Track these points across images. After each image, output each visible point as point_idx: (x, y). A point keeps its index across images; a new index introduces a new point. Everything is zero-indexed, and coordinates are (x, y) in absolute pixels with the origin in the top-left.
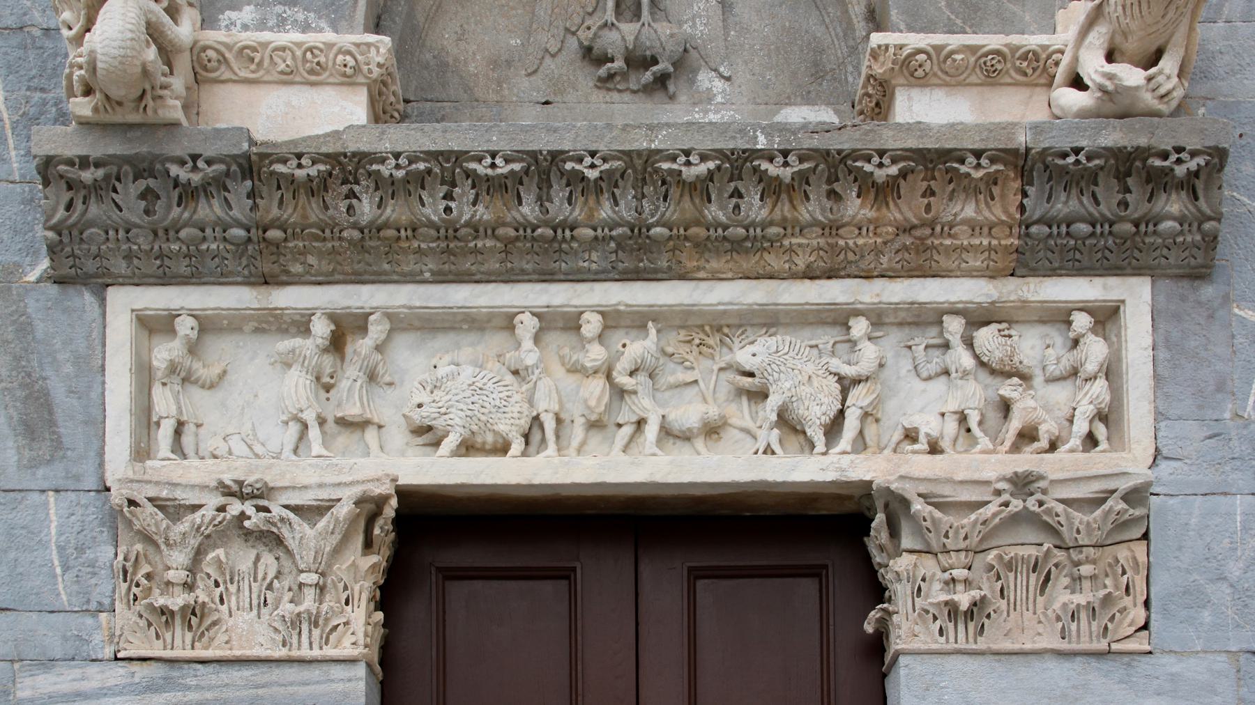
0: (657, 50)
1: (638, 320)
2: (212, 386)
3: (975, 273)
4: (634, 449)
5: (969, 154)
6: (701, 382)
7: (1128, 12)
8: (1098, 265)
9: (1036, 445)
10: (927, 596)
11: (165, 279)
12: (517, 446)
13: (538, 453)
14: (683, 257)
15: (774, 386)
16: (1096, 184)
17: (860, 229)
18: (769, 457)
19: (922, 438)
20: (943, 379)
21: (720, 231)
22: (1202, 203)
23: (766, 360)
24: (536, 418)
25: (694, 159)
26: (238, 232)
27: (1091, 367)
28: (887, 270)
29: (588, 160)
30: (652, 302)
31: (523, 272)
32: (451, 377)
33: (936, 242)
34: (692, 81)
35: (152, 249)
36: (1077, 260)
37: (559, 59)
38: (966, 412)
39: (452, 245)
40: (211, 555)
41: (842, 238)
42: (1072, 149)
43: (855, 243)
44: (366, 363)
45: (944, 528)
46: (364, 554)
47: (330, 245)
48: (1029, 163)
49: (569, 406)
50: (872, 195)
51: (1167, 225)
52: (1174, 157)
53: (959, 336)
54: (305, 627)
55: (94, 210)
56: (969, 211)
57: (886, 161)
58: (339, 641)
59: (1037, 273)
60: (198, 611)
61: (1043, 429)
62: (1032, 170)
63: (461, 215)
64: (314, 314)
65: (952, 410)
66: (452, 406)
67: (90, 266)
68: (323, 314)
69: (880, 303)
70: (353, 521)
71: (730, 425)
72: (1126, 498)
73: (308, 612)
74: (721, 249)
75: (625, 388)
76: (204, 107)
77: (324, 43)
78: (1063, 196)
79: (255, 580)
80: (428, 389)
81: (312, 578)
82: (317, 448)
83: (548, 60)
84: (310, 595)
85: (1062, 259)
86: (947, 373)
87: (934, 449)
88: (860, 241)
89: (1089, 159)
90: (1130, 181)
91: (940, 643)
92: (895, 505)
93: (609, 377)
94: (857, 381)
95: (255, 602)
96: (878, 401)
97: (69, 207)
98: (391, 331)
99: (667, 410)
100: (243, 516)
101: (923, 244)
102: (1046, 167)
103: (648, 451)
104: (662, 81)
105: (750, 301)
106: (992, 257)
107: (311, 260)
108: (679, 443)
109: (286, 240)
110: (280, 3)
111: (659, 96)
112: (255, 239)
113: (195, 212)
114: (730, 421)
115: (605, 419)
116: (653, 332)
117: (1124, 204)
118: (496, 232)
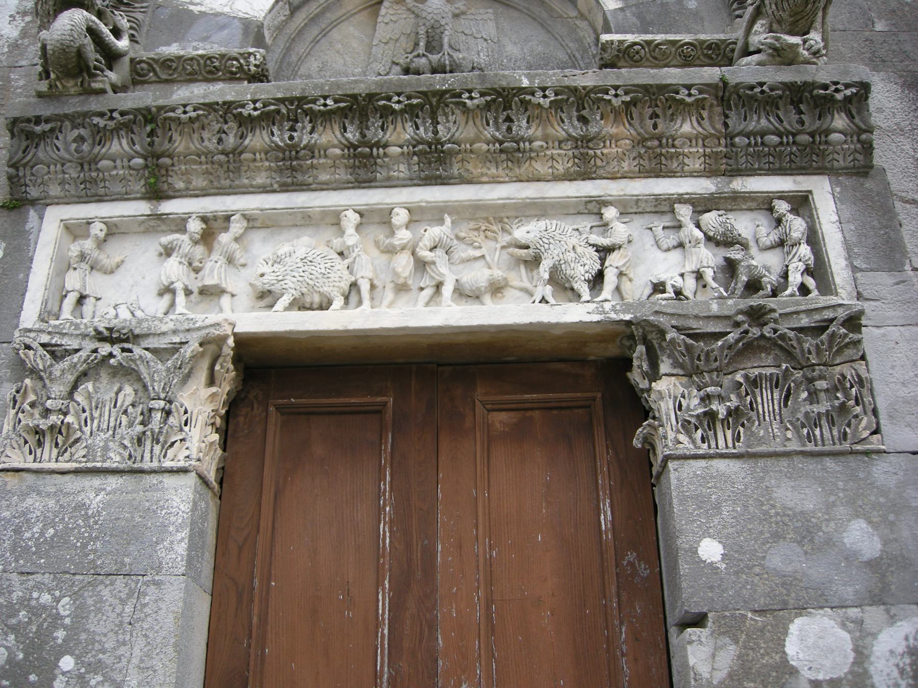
1: (436, 213)
2: (112, 272)
3: (696, 174)
5: (681, 88)
6: (488, 258)
7: (780, 7)
9: (761, 293)
12: (338, 302)
13: (357, 307)
14: (470, 167)
15: (546, 254)
16: (778, 109)
17: (604, 142)
18: (543, 305)
19: (669, 288)
20: (679, 251)
21: (497, 145)
23: (538, 235)
28: (626, 172)
29: (396, 98)
30: (446, 199)
32: (288, 255)
33: (664, 151)
35: (79, 176)
36: (771, 163)
38: (701, 270)
39: (294, 163)
41: (592, 149)
42: (757, 83)
43: (602, 153)
44: (225, 249)
47: (204, 167)
48: (727, 94)
50: (612, 116)
52: (833, 88)
53: (689, 218)
54: (148, 444)
56: (687, 128)
59: (742, 173)
60: (64, 431)
62: (729, 100)
63: (301, 140)
64: (190, 217)
65: (690, 270)
66: (287, 275)
68: (197, 217)
69: (625, 195)
71: (512, 287)
74: (498, 159)
75: (426, 260)
77: (219, 55)
79: (115, 406)
80: (270, 264)
85: (759, 163)
86: (681, 245)
89: (772, 90)
90: (802, 107)
92: (653, 337)
95: (112, 424)
98: (247, 229)
99: (460, 276)
100: (111, 355)
101: (653, 152)
102: (740, 97)
103: (443, 304)
105: (524, 196)
106: (707, 161)
109: (173, 165)
110: (196, 41)
112: (150, 164)
113: (109, 148)
114: (510, 283)
115: (410, 282)
116: (448, 220)
117: (802, 123)
118: (327, 152)
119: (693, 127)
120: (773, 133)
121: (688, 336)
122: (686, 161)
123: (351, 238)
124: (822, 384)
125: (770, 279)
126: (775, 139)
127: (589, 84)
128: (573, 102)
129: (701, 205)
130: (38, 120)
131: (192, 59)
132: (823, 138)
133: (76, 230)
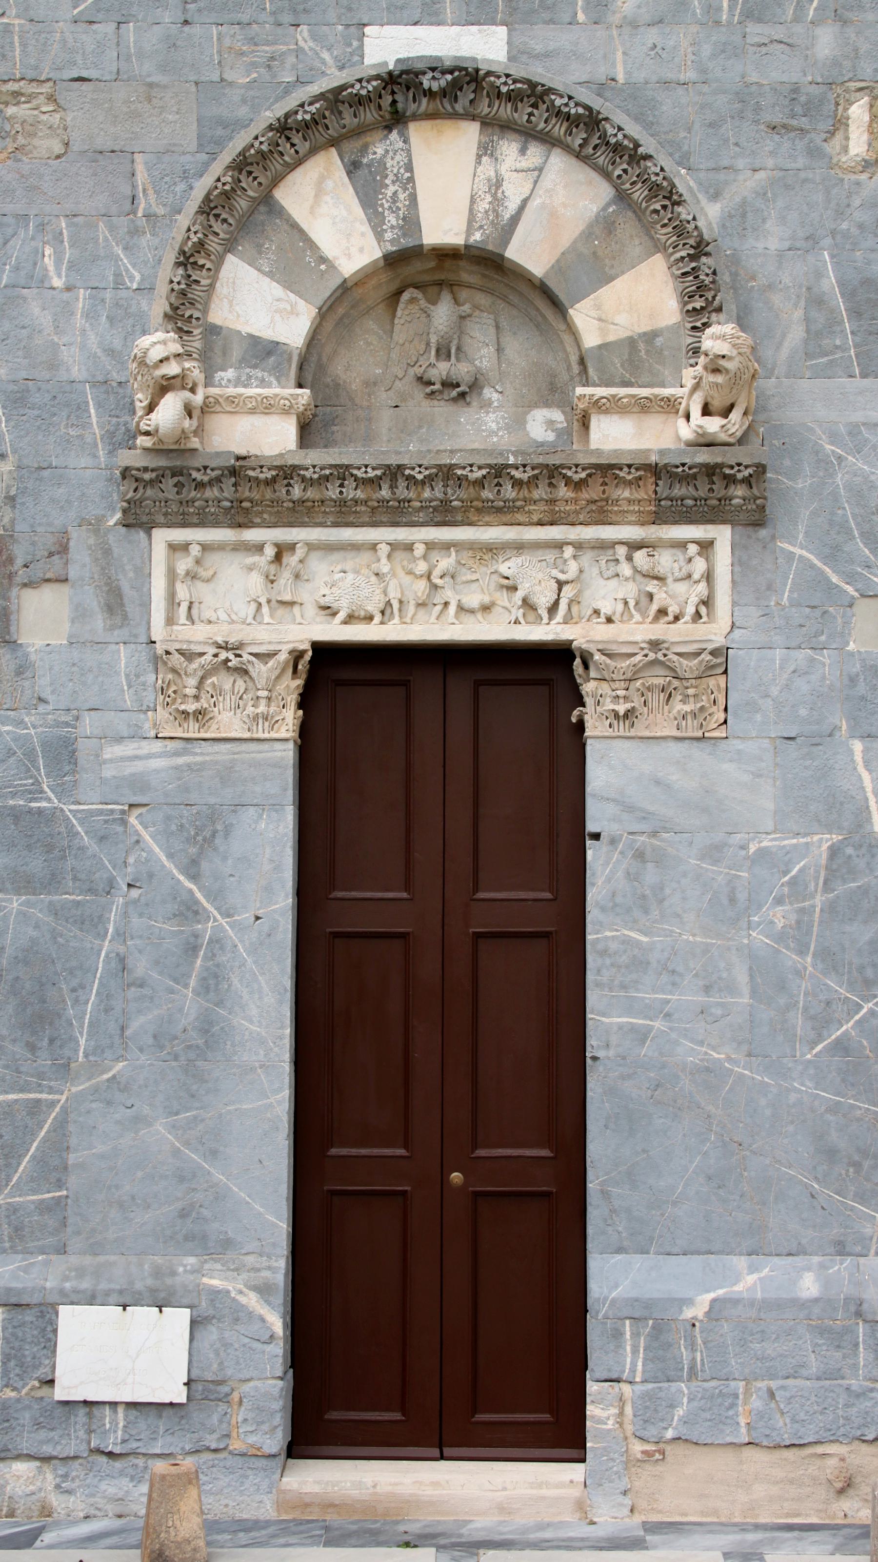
0: (460, 380)
4: (443, 618)
9: (667, 619)
10: (603, 705)
11: (184, 525)
12: (378, 618)
14: (470, 515)
22: (755, 491)
24: (389, 603)
25: (475, 469)
26: (227, 504)
27: (696, 576)
31: (382, 522)
34: (480, 394)
37: (403, 381)
40: (210, 681)
45: (612, 669)
46: (293, 679)
49: (406, 593)
51: (736, 501)
54: (260, 721)
55: (149, 492)
57: (579, 470)
58: (279, 729)
61: (670, 610)
67: (144, 519)
70: (286, 663)
72: (712, 653)
73: (263, 713)
76: (206, 427)
78: (678, 486)
81: (264, 693)
82: (267, 619)
83: (397, 382)
84: (263, 702)
87: (609, 620)
88: (568, 508)
91: (609, 732)
92: (586, 654)
93: (429, 578)
94: (567, 582)
96: (578, 595)
97: (135, 491)
100: (227, 660)
104: (463, 395)
107: (265, 516)
108: (468, 614)
111: (461, 402)
121: (609, 656)
123: (384, 567)
124: (691, 691)
125: (673, 610)
129: (635, 546)
130: (146, 469)
131: (251, 397)
133: (177, 548)
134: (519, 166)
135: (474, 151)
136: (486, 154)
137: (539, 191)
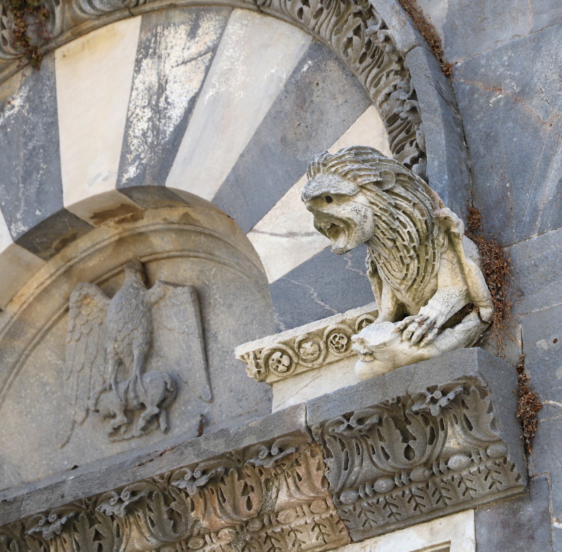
8: (418, 512)
119: (290, 496)
120: (382, 477)
122: (299, 536)
126: (382, 484)
127: (163, 471)
128: (157, 494)
132: (442, 467)
134: (187, 55)
135: (133, 56)
136: (145, 57)
137: (213, 78)
